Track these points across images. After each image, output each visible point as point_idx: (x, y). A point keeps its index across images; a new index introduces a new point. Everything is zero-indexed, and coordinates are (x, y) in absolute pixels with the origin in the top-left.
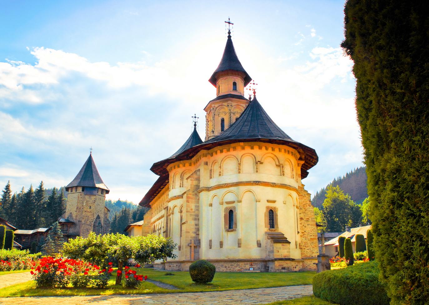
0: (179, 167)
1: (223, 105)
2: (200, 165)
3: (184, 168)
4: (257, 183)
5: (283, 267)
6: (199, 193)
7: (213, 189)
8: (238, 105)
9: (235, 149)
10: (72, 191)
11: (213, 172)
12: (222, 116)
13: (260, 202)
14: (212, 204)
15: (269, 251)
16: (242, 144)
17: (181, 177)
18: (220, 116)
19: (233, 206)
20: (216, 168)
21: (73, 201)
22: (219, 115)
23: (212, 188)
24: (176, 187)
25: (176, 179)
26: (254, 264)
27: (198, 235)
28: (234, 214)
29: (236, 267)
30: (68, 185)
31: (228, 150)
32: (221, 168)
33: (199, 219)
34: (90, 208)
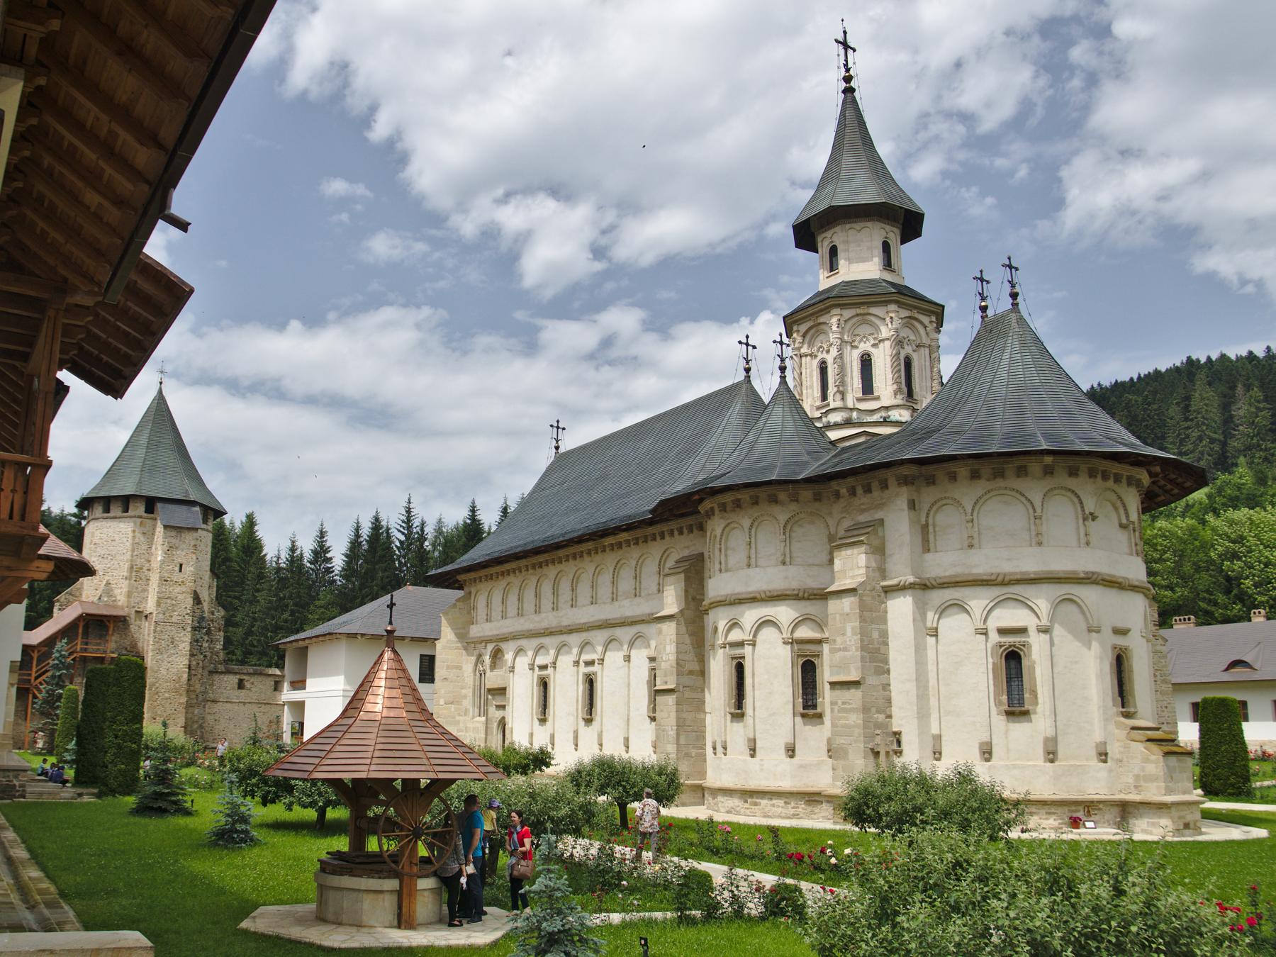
0: (774, 500)
1: (870, 314)
2: (880, 506)
3: (793, 506)
4: (1090, 579)
5: (1187, 821)
6: (886, 592)
7: (946, 585)
8: (909, 317)
9: (1022, 472)
10: (107, 510)
11: (935, 531)
12: (865, 347)
13: (1098, 632)
14: (936, 629)
15: (1137, 777)
16: (1048, 460)
17: (784, 533)
18: (856, 347)
19: (1023, 639)
20: (948, 519)
21: (113, 543)
22: (855, 344)
23: (941, 581)
24: (761, 562)
25: (759, 535)
26: (1096, 812)
27: (890, 717)
28: (1025, 663)
29: (1047, 819)
30: (94, 489)
31: (999, 474)
32: (976, 525)
33: (888, 672)
34: (180, 571)
